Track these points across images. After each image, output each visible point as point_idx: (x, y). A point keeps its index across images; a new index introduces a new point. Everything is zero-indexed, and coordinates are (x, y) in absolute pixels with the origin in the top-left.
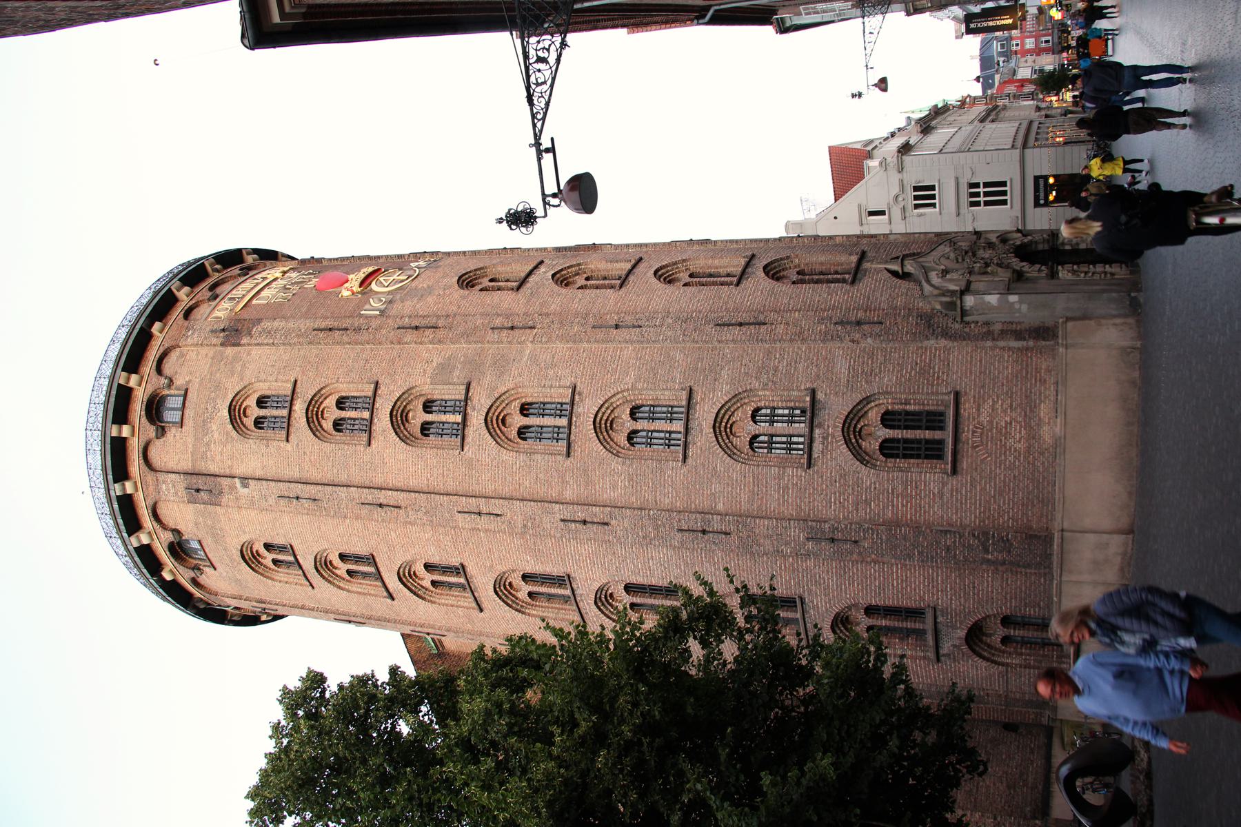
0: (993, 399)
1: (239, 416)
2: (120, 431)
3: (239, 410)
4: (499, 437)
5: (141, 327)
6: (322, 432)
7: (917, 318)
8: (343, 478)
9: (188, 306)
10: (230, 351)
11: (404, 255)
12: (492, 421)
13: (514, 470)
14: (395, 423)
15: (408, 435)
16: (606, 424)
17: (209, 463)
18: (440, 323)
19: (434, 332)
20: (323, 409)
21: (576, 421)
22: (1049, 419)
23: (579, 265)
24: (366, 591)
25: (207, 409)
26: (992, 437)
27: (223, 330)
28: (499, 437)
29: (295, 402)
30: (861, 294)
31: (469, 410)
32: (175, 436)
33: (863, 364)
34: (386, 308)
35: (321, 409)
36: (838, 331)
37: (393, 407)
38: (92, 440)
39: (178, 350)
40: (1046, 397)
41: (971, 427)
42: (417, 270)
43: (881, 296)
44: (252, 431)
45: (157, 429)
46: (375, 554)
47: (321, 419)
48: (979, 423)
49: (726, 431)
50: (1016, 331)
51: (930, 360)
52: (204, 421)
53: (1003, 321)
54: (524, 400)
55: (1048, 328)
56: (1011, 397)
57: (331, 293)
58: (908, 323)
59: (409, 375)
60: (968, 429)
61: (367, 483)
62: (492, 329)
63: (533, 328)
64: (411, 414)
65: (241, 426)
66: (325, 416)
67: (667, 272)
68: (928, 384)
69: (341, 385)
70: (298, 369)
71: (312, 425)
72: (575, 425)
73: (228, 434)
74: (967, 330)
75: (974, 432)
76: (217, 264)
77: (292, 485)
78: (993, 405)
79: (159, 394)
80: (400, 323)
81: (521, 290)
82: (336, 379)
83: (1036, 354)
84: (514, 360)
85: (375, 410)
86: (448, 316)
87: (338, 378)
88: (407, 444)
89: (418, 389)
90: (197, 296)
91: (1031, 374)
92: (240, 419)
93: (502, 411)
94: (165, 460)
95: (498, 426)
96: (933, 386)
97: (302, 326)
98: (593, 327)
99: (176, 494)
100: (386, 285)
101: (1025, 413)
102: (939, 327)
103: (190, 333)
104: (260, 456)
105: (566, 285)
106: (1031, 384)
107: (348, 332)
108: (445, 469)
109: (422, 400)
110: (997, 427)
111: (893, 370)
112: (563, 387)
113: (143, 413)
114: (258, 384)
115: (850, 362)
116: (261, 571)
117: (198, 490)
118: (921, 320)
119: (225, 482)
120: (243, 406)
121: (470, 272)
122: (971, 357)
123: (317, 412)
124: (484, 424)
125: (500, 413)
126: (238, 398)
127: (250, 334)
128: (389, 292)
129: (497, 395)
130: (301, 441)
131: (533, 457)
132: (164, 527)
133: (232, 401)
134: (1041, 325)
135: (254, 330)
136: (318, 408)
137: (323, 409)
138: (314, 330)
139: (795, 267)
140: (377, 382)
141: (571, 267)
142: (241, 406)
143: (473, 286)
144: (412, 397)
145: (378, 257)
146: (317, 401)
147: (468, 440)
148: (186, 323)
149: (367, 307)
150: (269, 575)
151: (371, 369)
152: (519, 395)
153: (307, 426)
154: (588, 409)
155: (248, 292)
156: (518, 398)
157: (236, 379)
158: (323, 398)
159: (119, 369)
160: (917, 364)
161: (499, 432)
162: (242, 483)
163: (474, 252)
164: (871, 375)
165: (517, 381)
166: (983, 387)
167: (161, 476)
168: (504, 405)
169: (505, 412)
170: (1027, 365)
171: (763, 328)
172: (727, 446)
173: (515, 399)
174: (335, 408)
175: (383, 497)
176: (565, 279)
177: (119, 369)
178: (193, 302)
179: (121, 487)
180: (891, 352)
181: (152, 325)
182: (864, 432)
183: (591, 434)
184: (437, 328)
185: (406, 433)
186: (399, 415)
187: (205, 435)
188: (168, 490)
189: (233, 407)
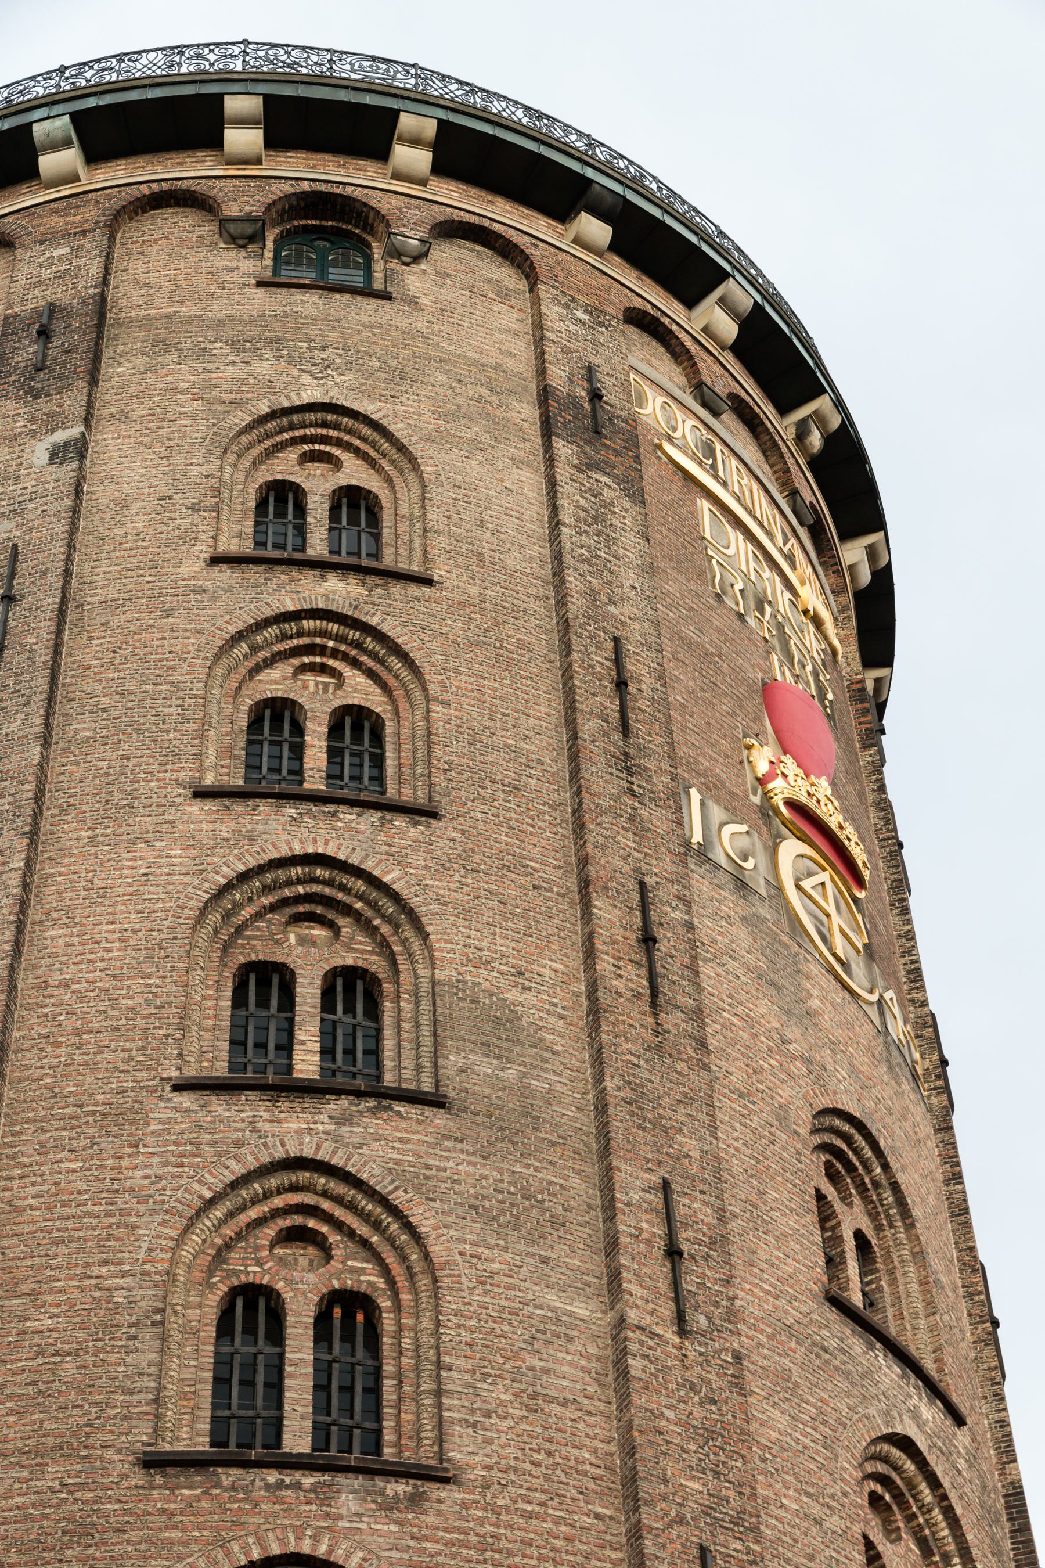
1: (304, 440)
2: (242, 122)
3: (325, 440)
4: (231, 1215)
5: (590, 182)
6: (249, 664)
9: (674, 327)
11: (922, 988)
12: (295, 1188)
13: (95, 1270)
14: (281, 874)
15: (237, 920)
17: (140, 361)
18: (673, 1020)
19: (638, 996)
20: (333, 672)
21: (297, 1486)
25: (324, 348)
27: (596, 396)
28: (231, 1215)
29: (353, 580)
31: (336, 1105)
32: (231, 270)
34: (718, 867)
35: (331, 662)
37: (344, 867)
38: (212, 57)
39: (523, 285)
42: (874, 998)
44: (248, 473)
45: (255, 220)
47: (296, 662)
52: (280, 341)
54: (385, 1303)
57: (757, 720)
59: (466, 914)
61: (53, 799)
62: (666, 1186)
63: (683, 1331)
64: (319, 932)
65: (269, 443)
66: (310, 678)
69: (420, 713)
70: (475, 591)
71: (273, 631)
72: (280, 1485)
76: (830, 439)
77: (55, 581)
79: (372, 232)
80: (664, 893)
81: (832, 1315)
82: (445, 696)
84: (545, 1260)
85: (330, 808)
86: (702, 1044)
87: (445, 703)
88: (203, 912)
89: (416, 945)
90: (709, 359)
92: (294, 442)
93: (338, 1225)
95: (276, 1213)
97: (628, 609)
98: (703, 1550)
99: (38, 284)
100: (807, 884)
103: (581, 315)
104: (162, 491)
105: (874, 1499)
107: (616, 737)
108: (106, 1037)
109: (376, 964)
112: (440, 1441)
114: (415, 487)
117: (44, 334)
119: (73, 401)
120: (337, 452)
121: (886, 1167)
123: (322, 650)
124: (279, 1153)
125: (328, 1218)
127: (588, 466)
128: (780, 889)
129: (399, 1198)
130: (214, 598)
131: (147, 1334)
133: (354, 415)
135: (604, 479)
136: (335, 653)
137: (333, 672)
138: (616, 640)
140: (434, 815)
141: (954, 1522)
142: (339, 443)
143: (832, 1176)
144: (385, 929)
145: (905, 911)
146: (358, 645)
147: (219, 1106)
148: (614, 311)
149: (717, 813)
151: (484, 801)
152: (402, 1282)
153: (269, 613)
154: (348, 1533)
155: (738, 499)
156: (391, 1282)
157: (430, 423)
158: (371, 664)
159: (442, 114)
161: (253, 1214)
162: (67, 445)
163: (965, 1211)
165: (462, 1268)
167: (94, 243)
168: (363, 1230)
169: (334, 1238)
173: (386, 1271)
174: (337, 703)
176: (898, 1496)
177: (442, 114)
178: (689, 344)
179: (59, 135)
181: (603, 216)
183: (245, 1549)
184: (654, 1004)
185: (246, 913)
186: (316, 888)
187: (233, 344)
188: (51, 262)
189: (331, 417)
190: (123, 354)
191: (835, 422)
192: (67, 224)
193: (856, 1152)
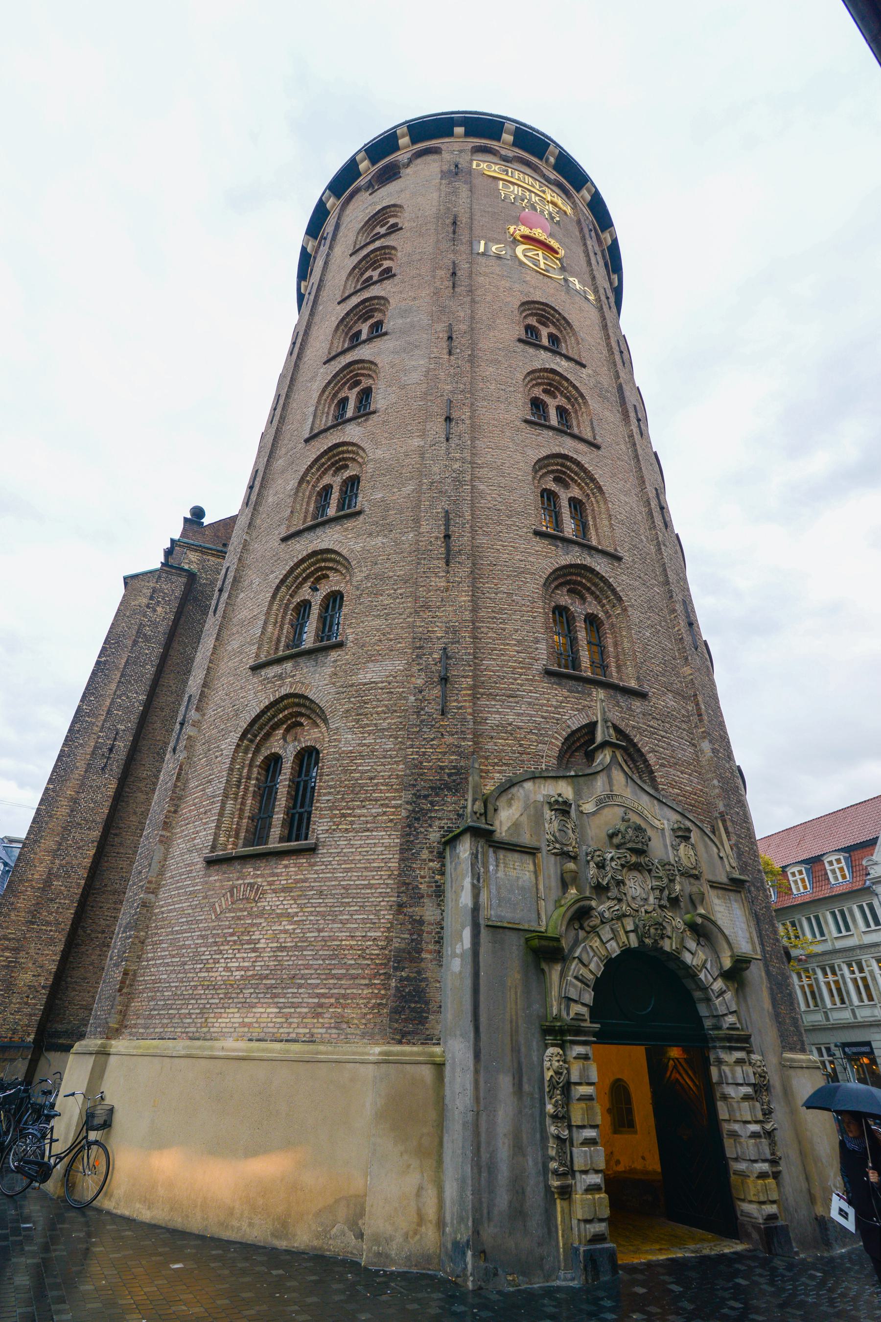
0: (296, 914)
7: (455, 767)
16: (340, 460)
22: (249, 1025)
23: (582, 396)
26: (239, 918)
28: (336, 384)
30: (522, 685)
33: (378, 700)
36: (431, 654)
40: (287, 1016)
41: (259, 880)
43: (519, 715)
48: (264, 892)
49: (317, 570)
50: (419, 951)
51: (376, 800)
53: (445, 924)
55: (423, 1021)
56: (296, 946)
58: (444, 753)
60: (258, 876)
67: (576, 474)
68: (336, 800)
74: (425, 855)
75: (252, 885)
78: (288, 915)
83: (376, 996)
91: (335, 986)
95: (348, 380)
96: (331, 809)
101: (266, 977)
102: (432, 803)
106: (317, 986)
110: (252, 925)
111: (365, 745)
115: (382, 682)
118: (450, 775)
121: (560, 314)
122: (379, 869)
126: (392, 209)
134: (433, 1006)
139: (606, 612)
147: (333, 363)
160: (371, 779)
164: (361, 715)
166: (321, 893)
170: (354, 977)
171: (442, 563)
172: (297, 578)
180: (396, 738)
181: (460, 126)
182: (299, 729)
191: (557, 152)
193: (548, 313)
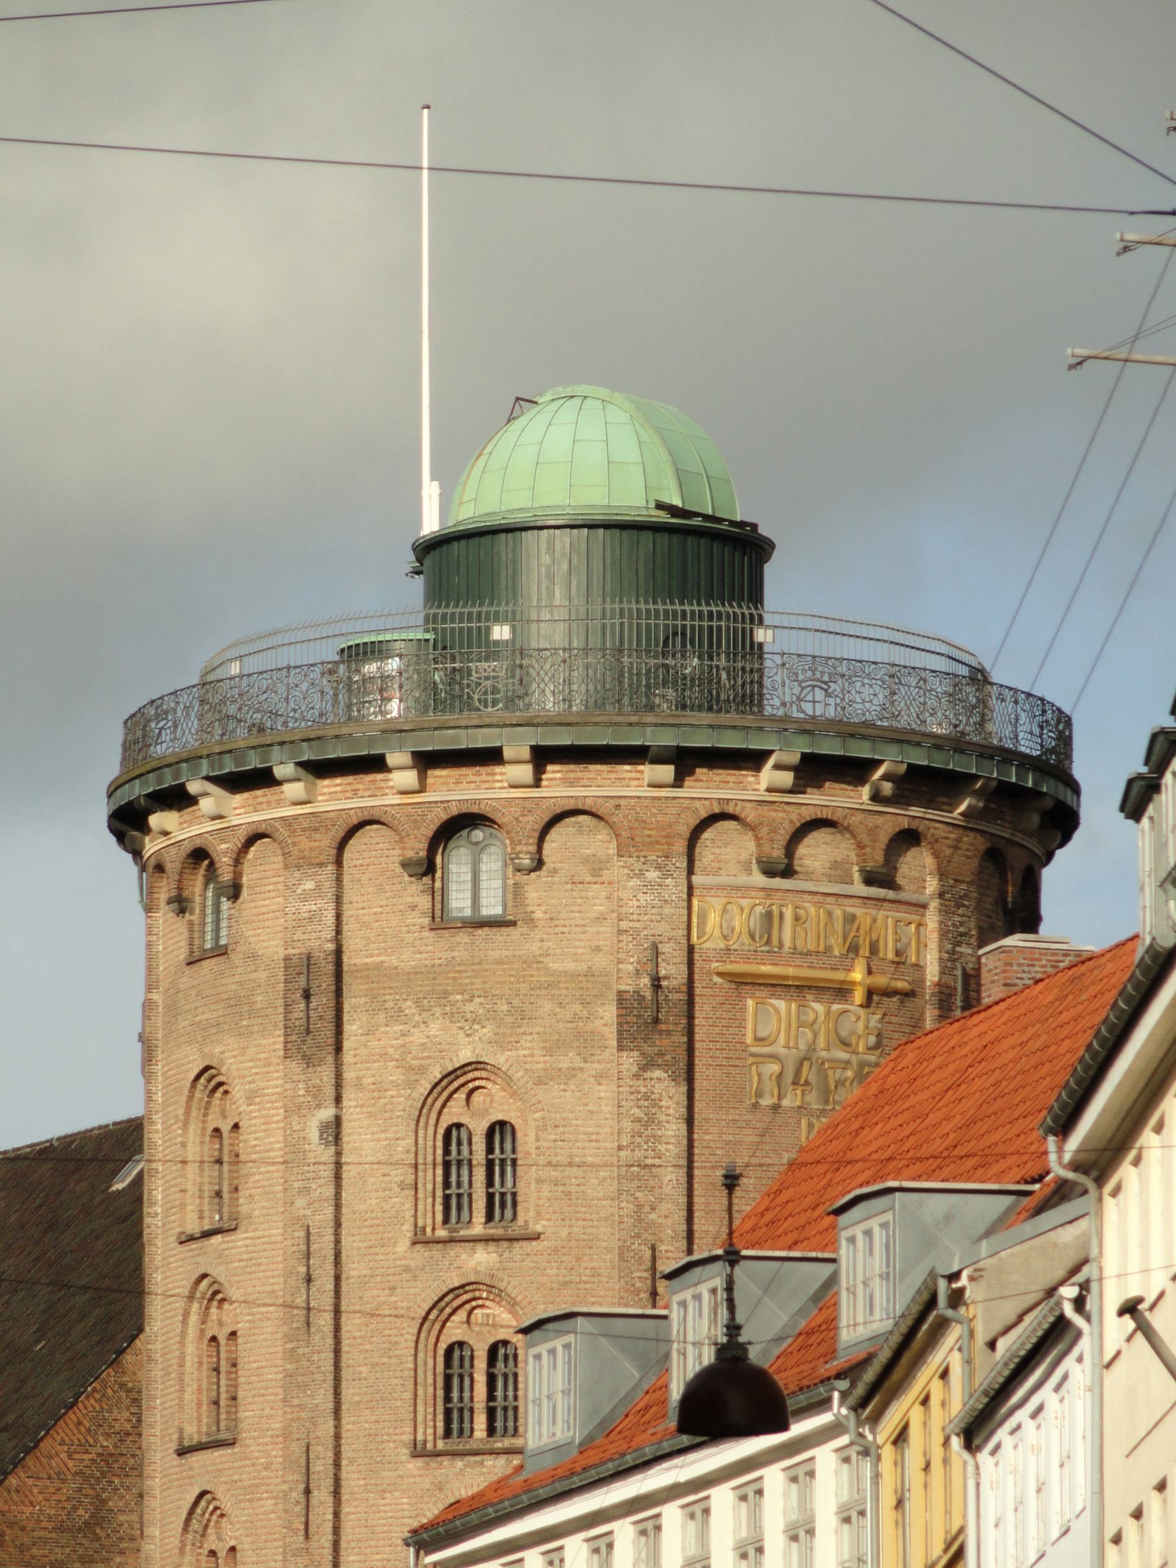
8: (349, 1393)
10: (609, 1013)
24: (187, 1378)
29: (491, 1247)
46: (237, 1449)
65: (445, 1094)
70: (564, 1233)
73: (423, 1070)
85: (478, 1458)
92: (463, 1085)
94: (365, 878)
103: (653, 875)
113: (455, 812)
116: (198, 1095)
117: (307, 995)
119: (326, 1074)
130: (415, 1278)
132: (238, 860)
135: (658, 1073)
138: (653, 1248)
150: (194, 1113)
175: (322, 1496)
187: (417, 1002)
190: (355, 1008)
192: (311, 849)
